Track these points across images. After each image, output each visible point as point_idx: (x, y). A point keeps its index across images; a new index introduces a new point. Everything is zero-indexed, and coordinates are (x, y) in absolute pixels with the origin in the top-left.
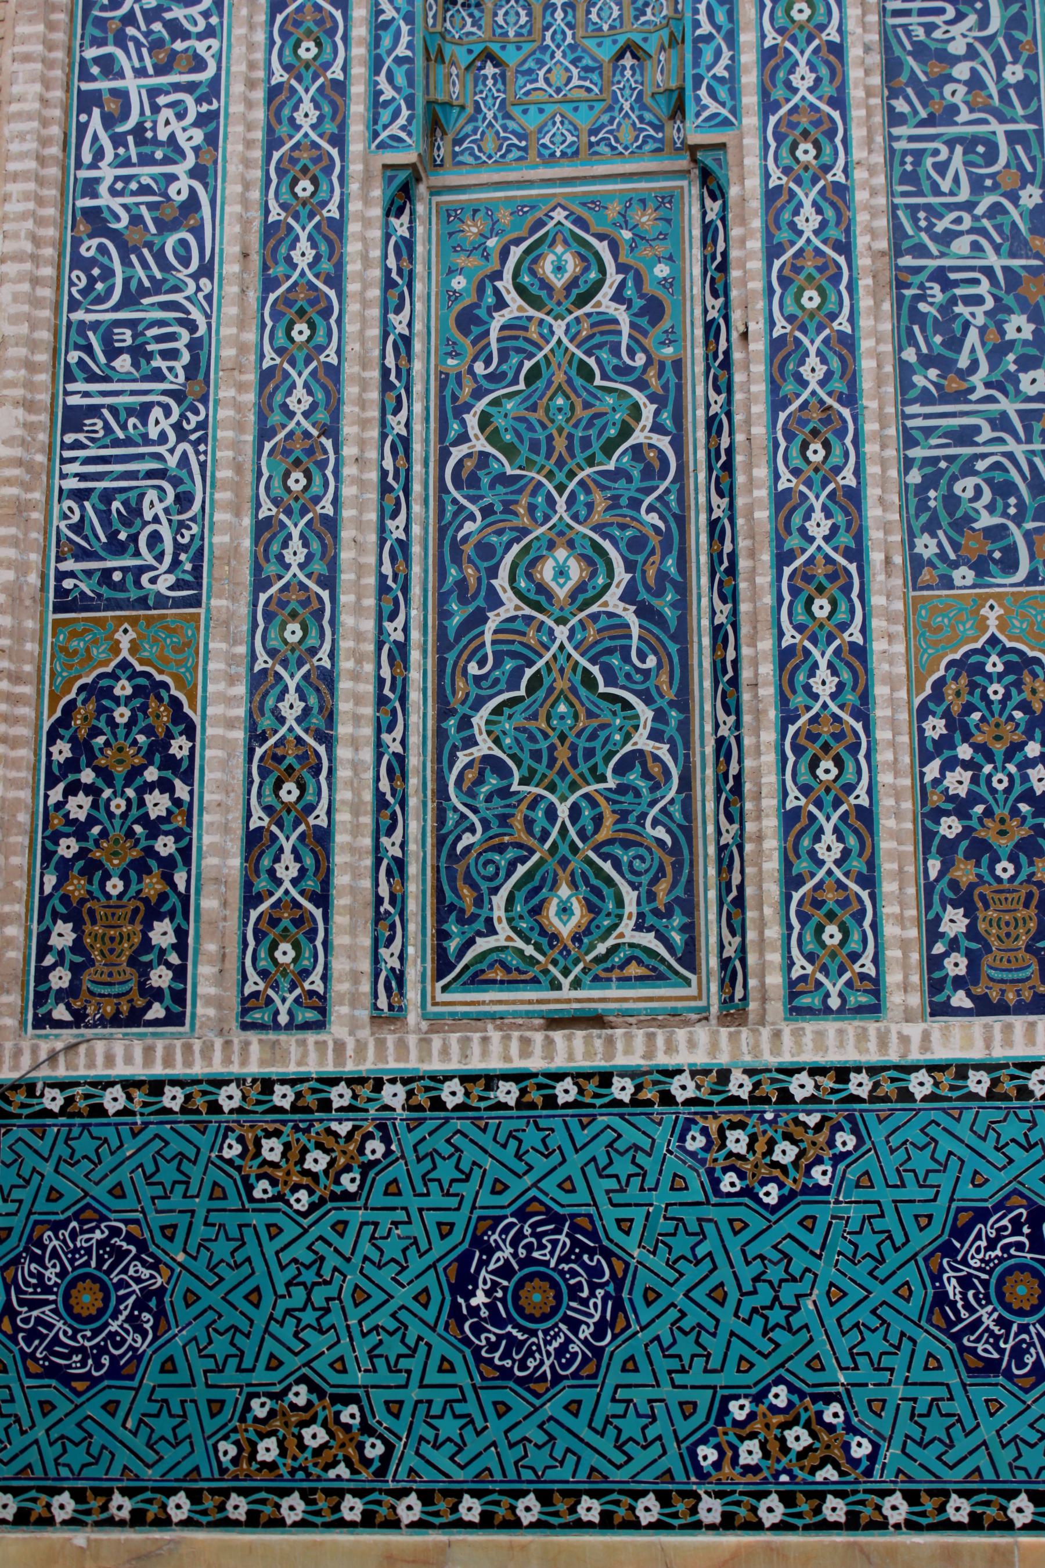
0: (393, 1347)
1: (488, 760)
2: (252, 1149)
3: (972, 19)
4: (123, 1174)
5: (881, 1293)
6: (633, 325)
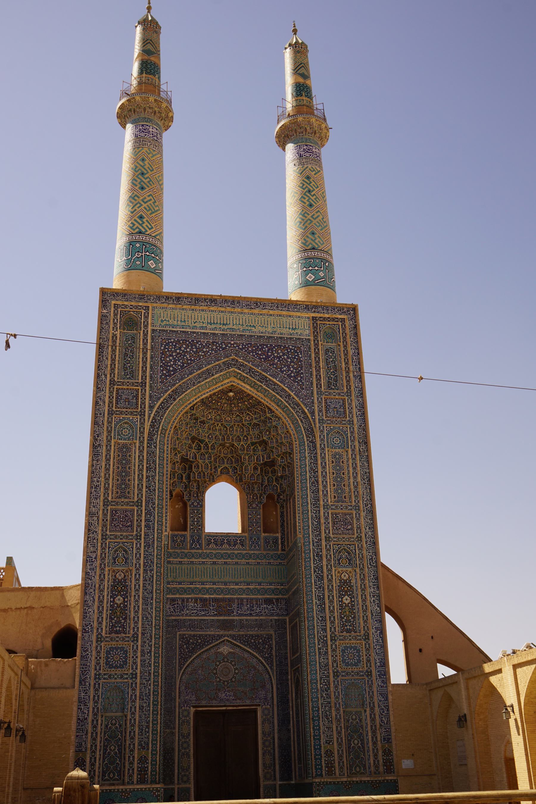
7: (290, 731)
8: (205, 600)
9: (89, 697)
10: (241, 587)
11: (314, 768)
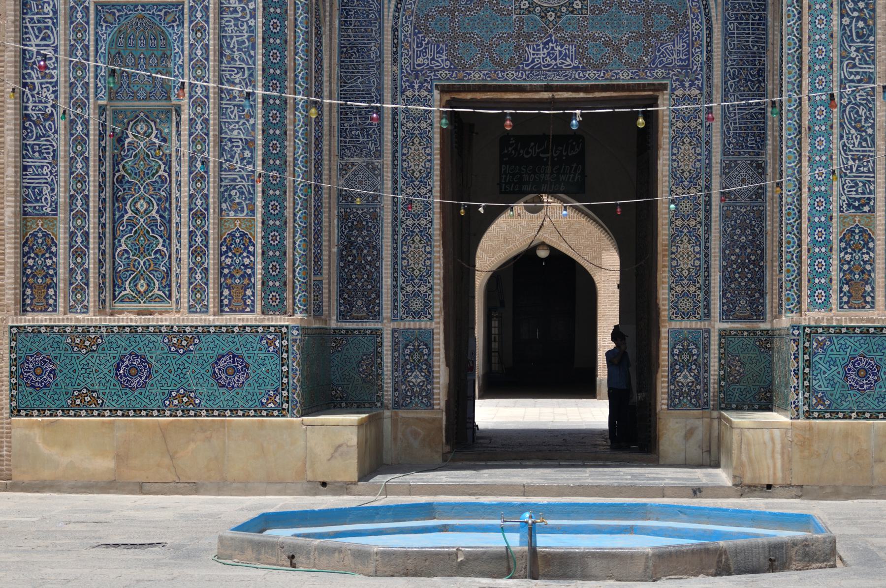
0: (104, 381)
1: (125, 250)
2: (73, 341)
3: (241, 74)
4: (46, 346)
5: (203, 371)
7: (764, 169)
9: (56, 50)
11: (805, 283)
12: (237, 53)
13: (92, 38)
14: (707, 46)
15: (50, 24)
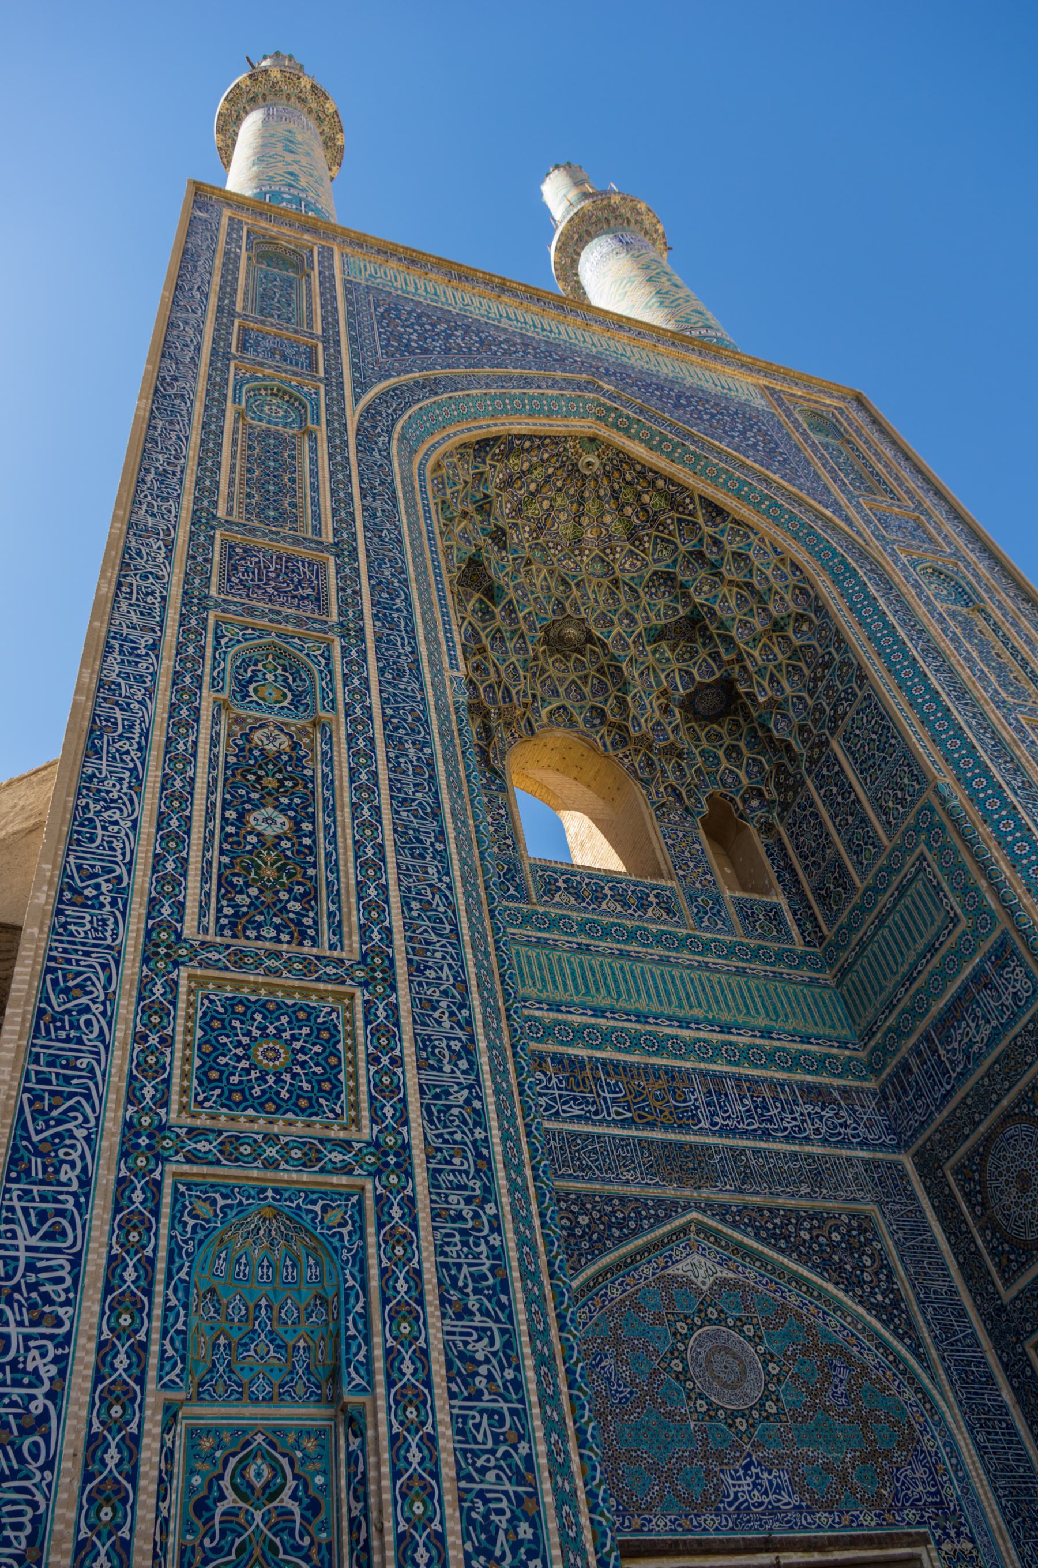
3: (486, 1341)
6: (303, 1517)
8: (575, 1064)
9: (76, 1261)
10: (702, 1035)
12: (472, 1297)
13: (163, 1243)
14: (956, 1472)
15: (70, 1205)
